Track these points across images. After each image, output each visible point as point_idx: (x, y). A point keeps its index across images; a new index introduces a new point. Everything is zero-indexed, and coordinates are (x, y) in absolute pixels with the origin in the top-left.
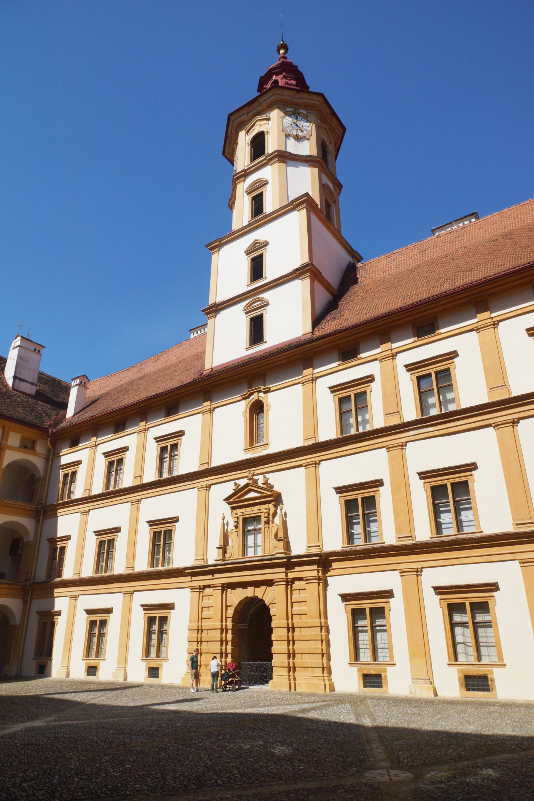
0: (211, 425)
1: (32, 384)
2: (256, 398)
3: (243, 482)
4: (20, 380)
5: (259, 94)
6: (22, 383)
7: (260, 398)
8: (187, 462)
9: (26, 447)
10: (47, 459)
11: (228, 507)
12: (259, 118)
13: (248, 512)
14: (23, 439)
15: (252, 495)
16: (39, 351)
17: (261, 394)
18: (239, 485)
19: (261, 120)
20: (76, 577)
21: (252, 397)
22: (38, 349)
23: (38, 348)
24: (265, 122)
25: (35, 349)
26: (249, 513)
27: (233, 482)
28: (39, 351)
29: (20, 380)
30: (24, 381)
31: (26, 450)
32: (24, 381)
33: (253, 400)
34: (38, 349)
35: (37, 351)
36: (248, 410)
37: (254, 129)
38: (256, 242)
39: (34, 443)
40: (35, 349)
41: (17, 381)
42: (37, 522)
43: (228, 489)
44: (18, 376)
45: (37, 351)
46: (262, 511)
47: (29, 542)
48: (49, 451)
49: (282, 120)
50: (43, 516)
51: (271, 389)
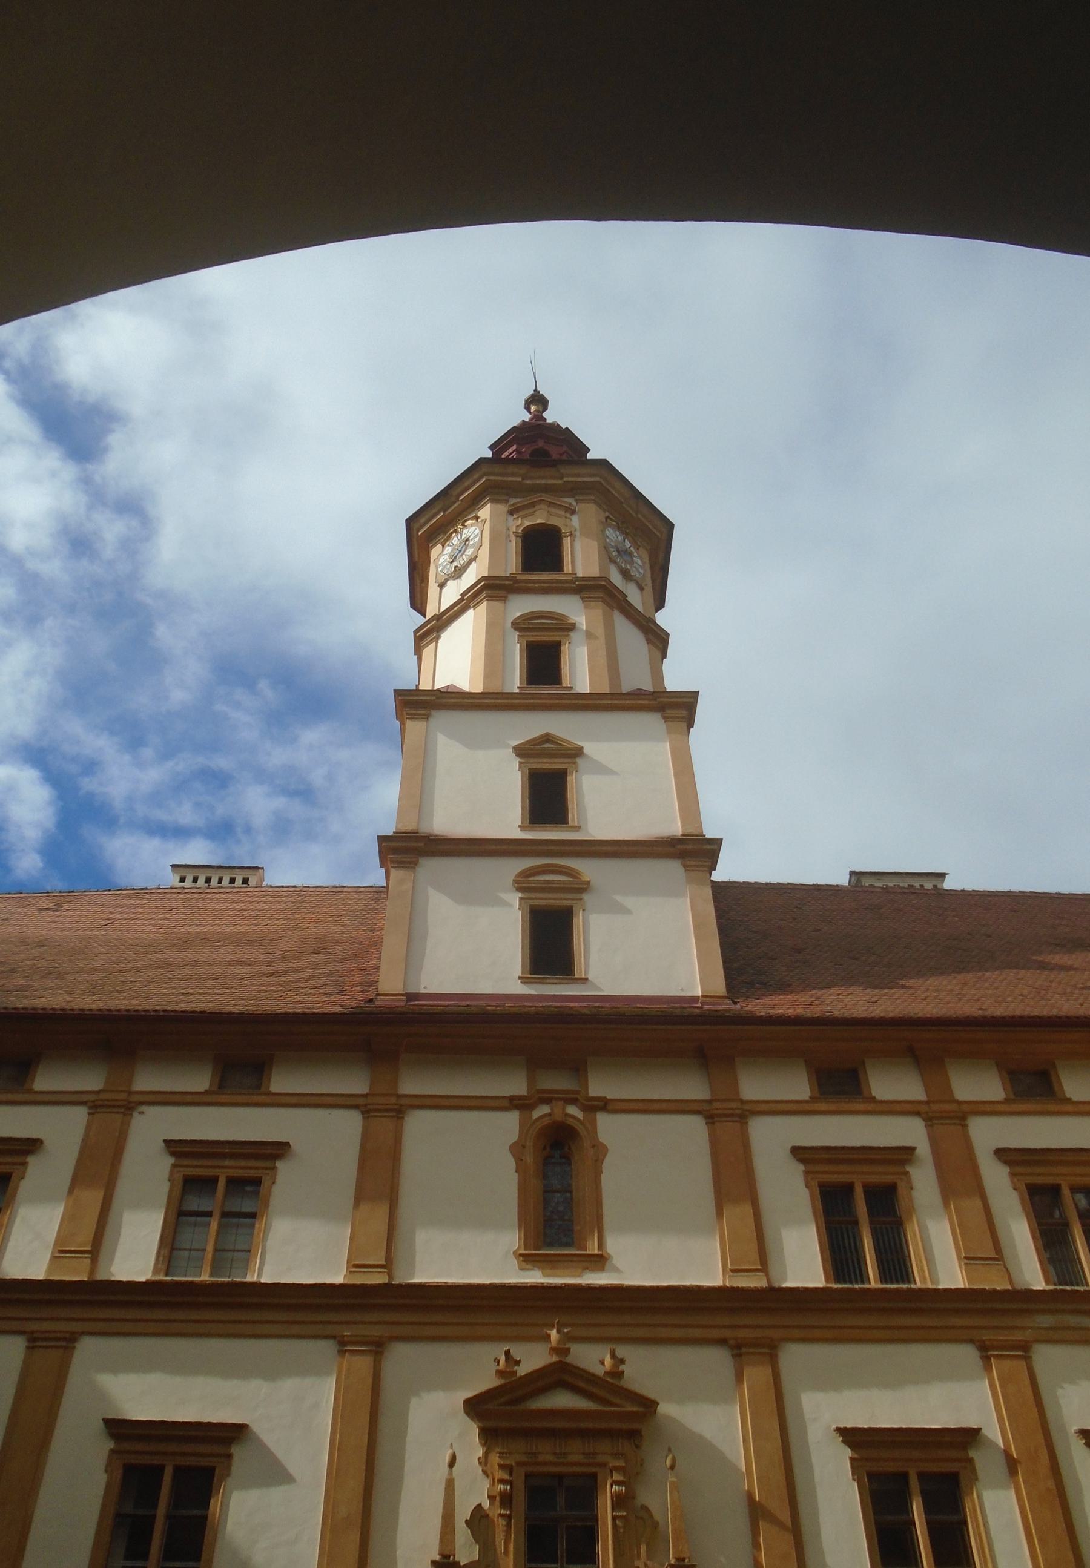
0: (395, 1155)
2: (558, 1117)
3: (532, 1358)
5: (489, 454)
7: (570, 1121)
8: (301, 1247)
11: (473, 1430)
12: (545, 497)
13: (546, 1453)
15: (563, 1400)
17: (573, 1110)
18: (518, 1363)
19: (551, 504)
21: (545, 1109)
24: (562, 513)
26: (550, 1458)
27: (498, 1351)
33: (547, 1120)
36: (529, 1144)
37: (533, 514)
38: (547, 738)
43: (479, 1367)
46: (601, 1459)
49: (603, 531)
51: (610, 1107)
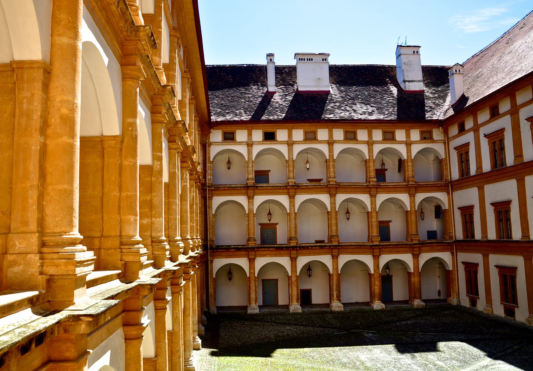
1: (419, 81)
4: (409, 81)
6: (410, 83)
9: (425, 138)
10: (445, 143)
14: (422, 133)
16: (417, 52)
20: (485, 239)
22: (415, 50)
23: (415, 49)
25: (414, 52)
28: (417, 52)
29: (409, 81)
30: (412, 81)
31: (426, 141)
32: (412, 81)
34: (415, 50)
35: (416, 52)
39: (431, 133)
40: (414, 52)
41: (407, 83)
42: (448, 193)
44: (406, 79)
45: (416, 52)
47: (446, 210)
48: (445, 136)
50: (452, 191)
